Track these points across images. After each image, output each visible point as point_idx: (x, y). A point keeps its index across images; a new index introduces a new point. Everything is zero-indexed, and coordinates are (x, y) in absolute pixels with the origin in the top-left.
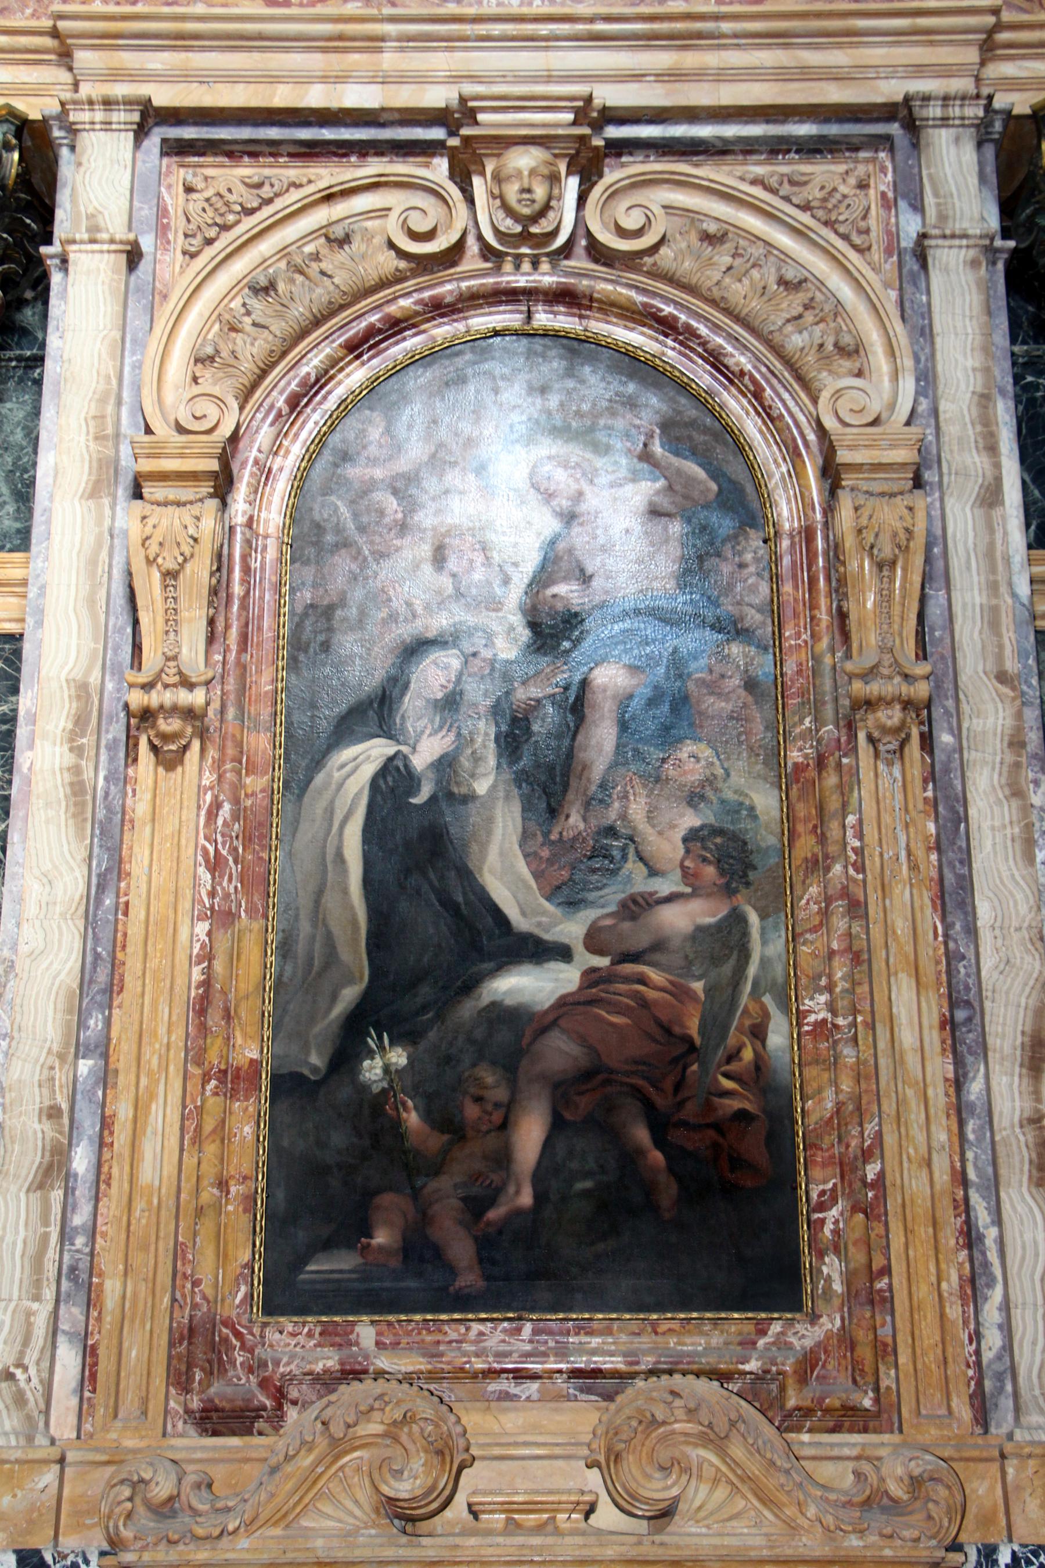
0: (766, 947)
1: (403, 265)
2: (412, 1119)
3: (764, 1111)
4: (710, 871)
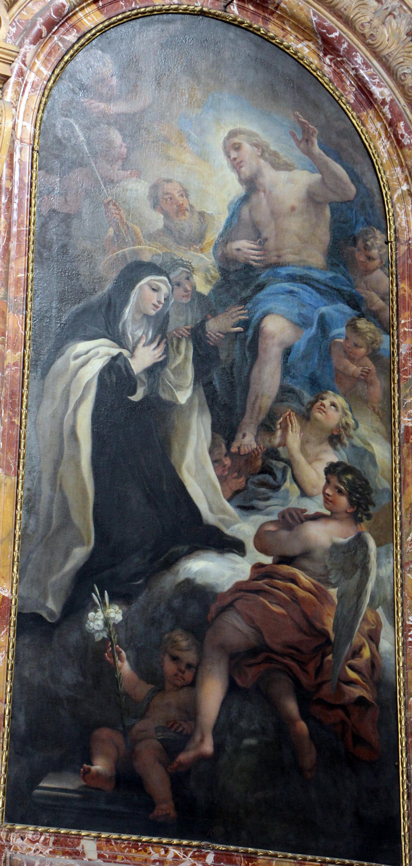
2: (125, 667)
3: (377, 701)
4: (343, 501)
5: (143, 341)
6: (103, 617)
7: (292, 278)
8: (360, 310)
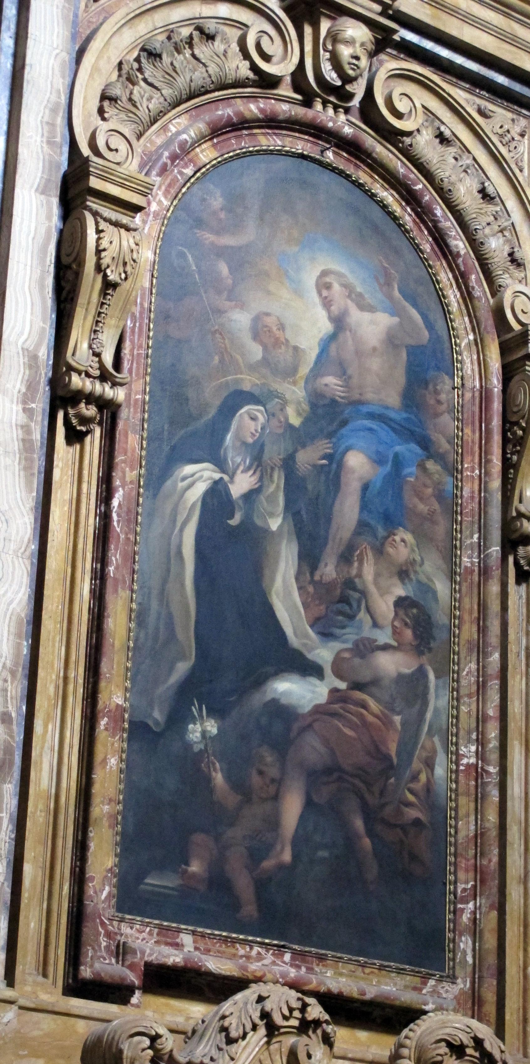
0: (438, 701)
1: (251, 75)
2: (219, 778)
4: (408, 633)
5: (241, 468)
6: (202, 729)
8: (429, 452)
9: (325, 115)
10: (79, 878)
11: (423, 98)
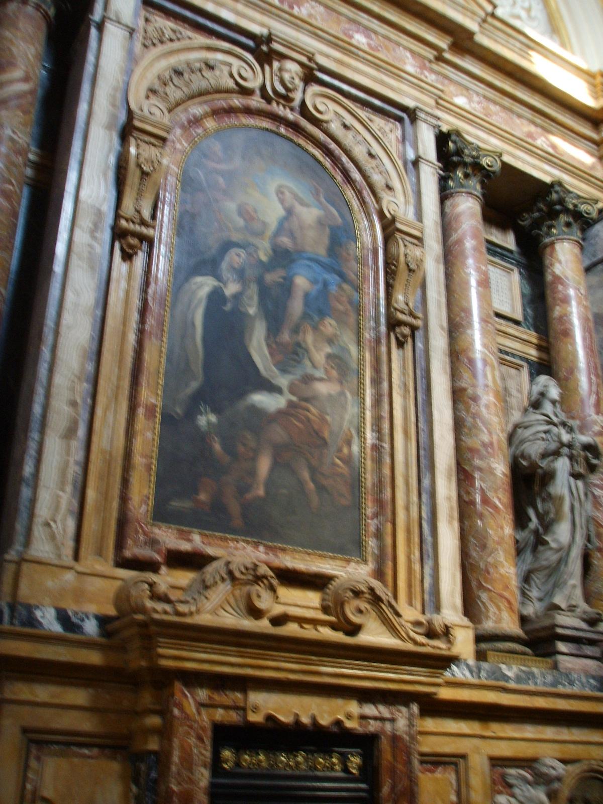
1: (235, 87)
2: (217, 447)
6: (206, 419)
7: (310, 259)
9: (281, 111)
10: (124, 499)
11: (332, 106)
